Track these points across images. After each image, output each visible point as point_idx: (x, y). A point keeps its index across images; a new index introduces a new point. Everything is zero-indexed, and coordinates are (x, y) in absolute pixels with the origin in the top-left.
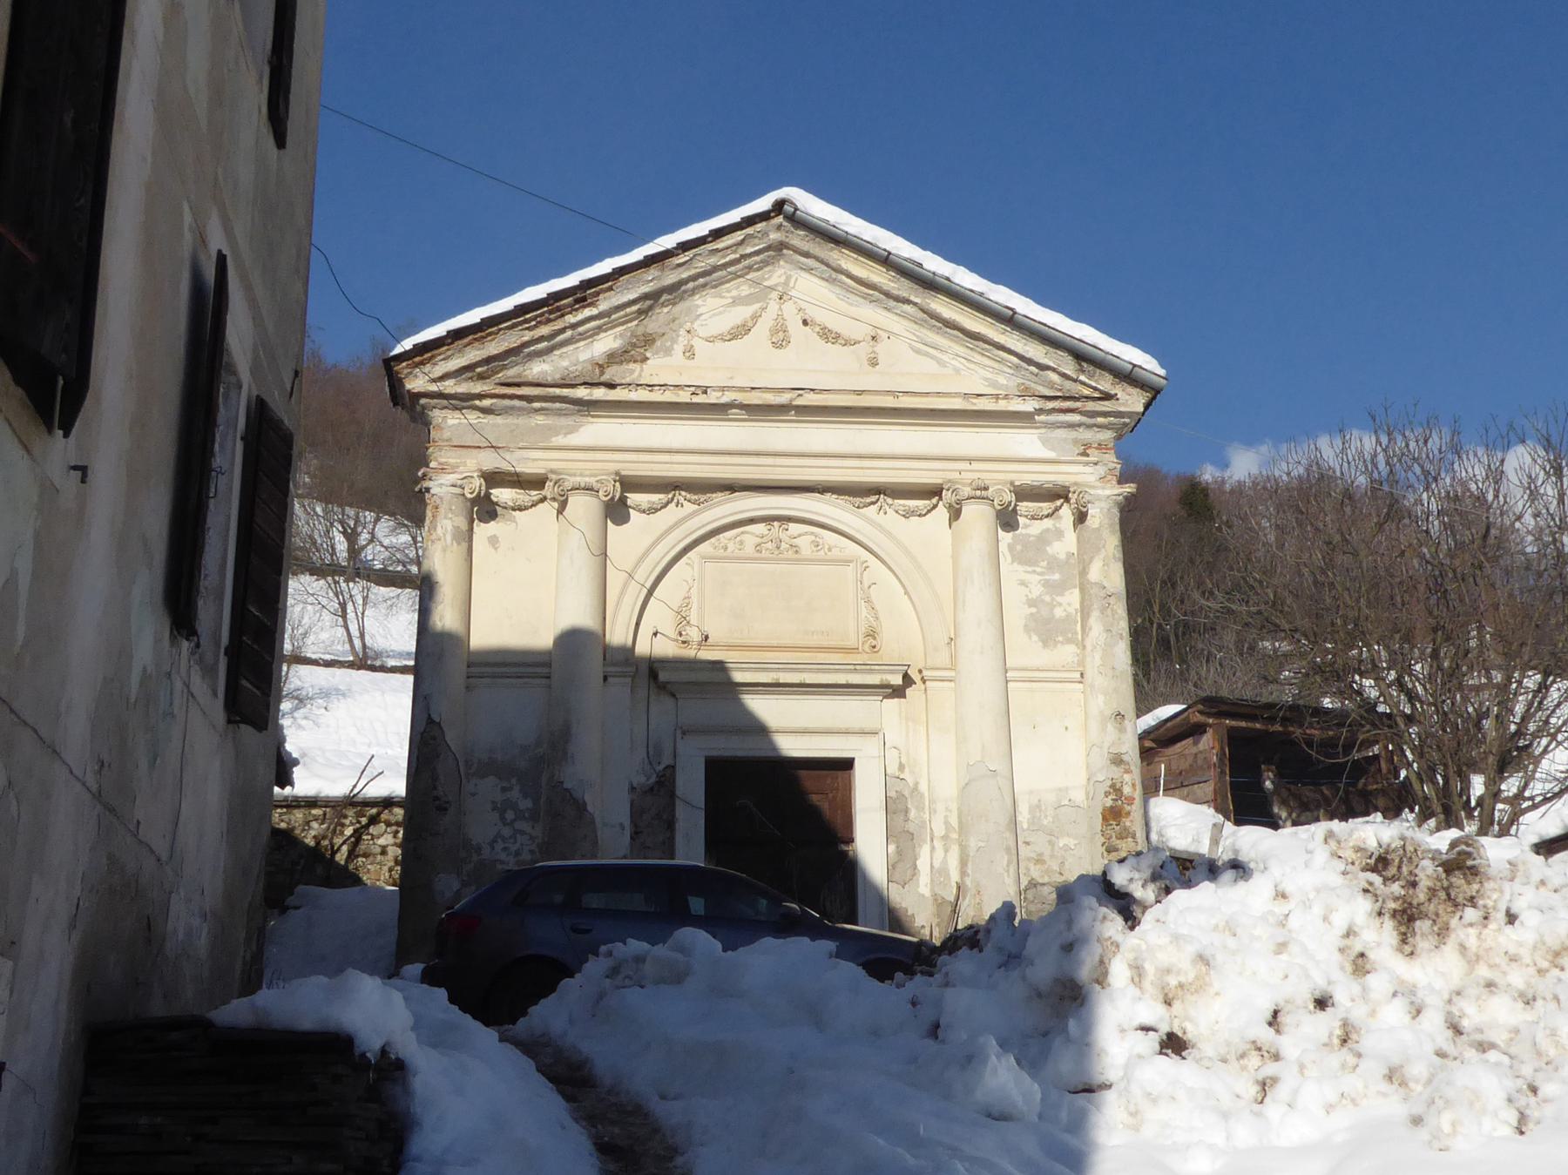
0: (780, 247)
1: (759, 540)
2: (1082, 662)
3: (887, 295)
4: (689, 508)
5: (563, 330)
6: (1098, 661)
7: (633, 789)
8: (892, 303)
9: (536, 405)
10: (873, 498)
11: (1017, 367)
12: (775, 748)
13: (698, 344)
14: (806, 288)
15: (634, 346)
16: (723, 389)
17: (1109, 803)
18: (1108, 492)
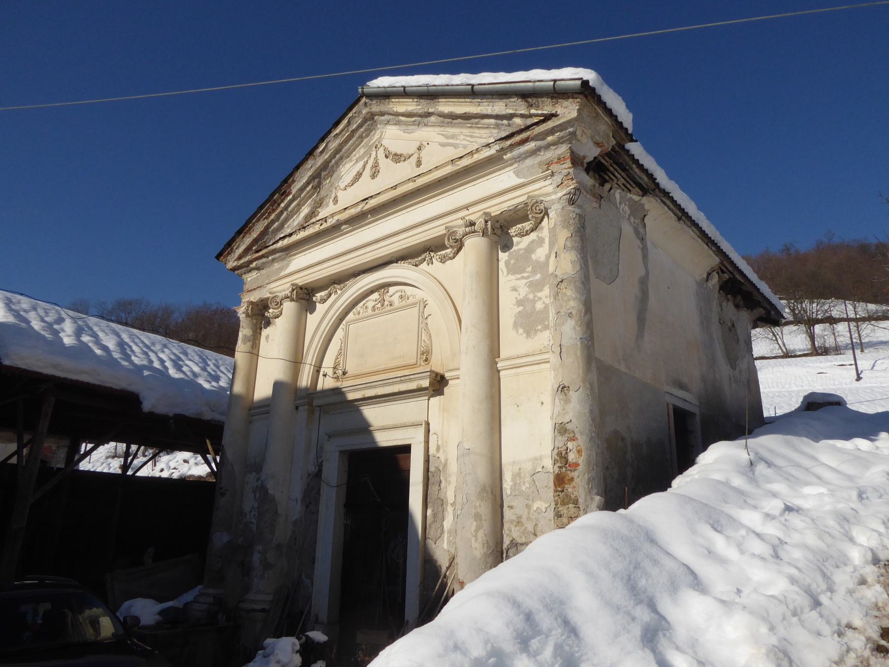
0: (371, 116)
1: (374, 303)
3: (421, 116)
4: (339, 292)
5: (282, 212)
7: (309, 475)
8: (425, 120)
10: (423, 256)
11: (497, 126)
18: (559, 195)
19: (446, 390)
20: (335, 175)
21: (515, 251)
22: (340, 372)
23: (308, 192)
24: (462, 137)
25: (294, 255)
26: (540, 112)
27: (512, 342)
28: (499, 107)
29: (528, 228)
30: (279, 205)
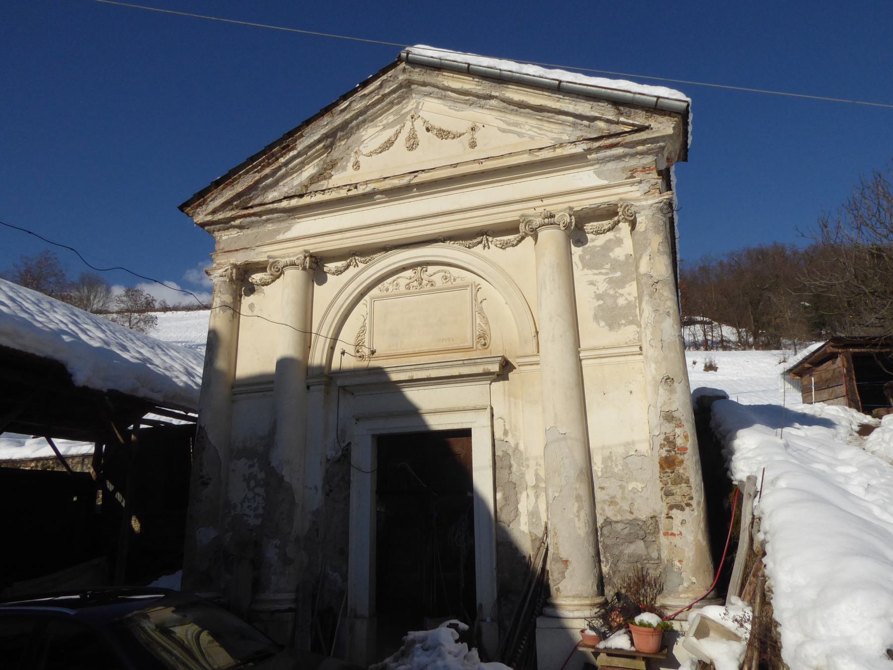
1: (408, 281)
2: (640, 340)
3: (478, 96)
5: (279, 168)
6: (649, 337)
7: (328, 460)
8: (483, 102)
9: (264, 217)
10: (479, 239)
11: (574, 125)
12: (425, 425)
13: (362, 159)
14: (430, 109)
15: (325, 169)
16: (366, 183)
17: (664, 454)
18: (650, 202)
19: (511, 375)
21: (590, 247)
22: (366, 351)
24: (527, 127)
26: (631, 122)
27: (593, 334)
28: (584, 108)
29: (606, 227)
30: (277, 159)
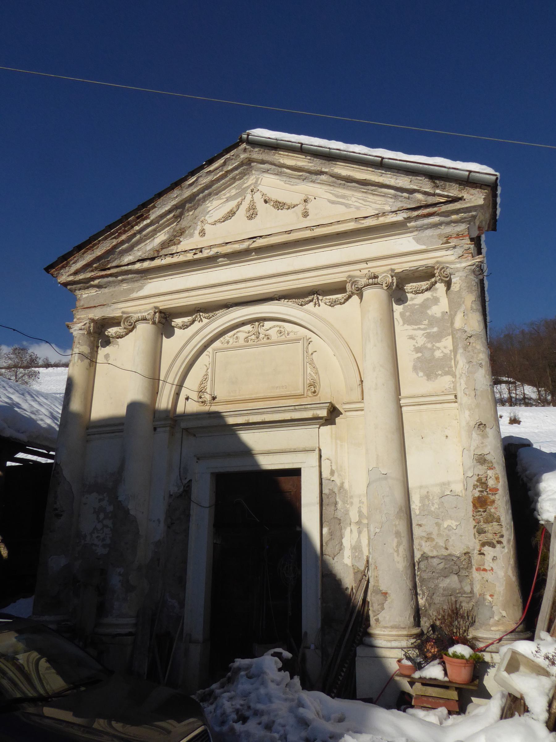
0: (249, 162)
1: (247, 335)
2: (455, 388)
4: (205, 321)
5: (134, 235)
6: (463, 386)
8: (314, 177)
9: (120, 278)
10: (310, 298)
11: (395, 197)
13: (207, 227)
14: (269, 184)
15: (175, 236)
16: (210, 247)
17: (477, 494)
18: (464, 265)
19: (338, 420)
20: (200, 209)
21: (409, 305)
22: (208, 397)
23: (168, 220)
24: (353, 199)
25: (150, 279)
26: (446, 193)
27: (413, 383)
28: (403, 181)
29: (424, 287)
30: (132, 227)
